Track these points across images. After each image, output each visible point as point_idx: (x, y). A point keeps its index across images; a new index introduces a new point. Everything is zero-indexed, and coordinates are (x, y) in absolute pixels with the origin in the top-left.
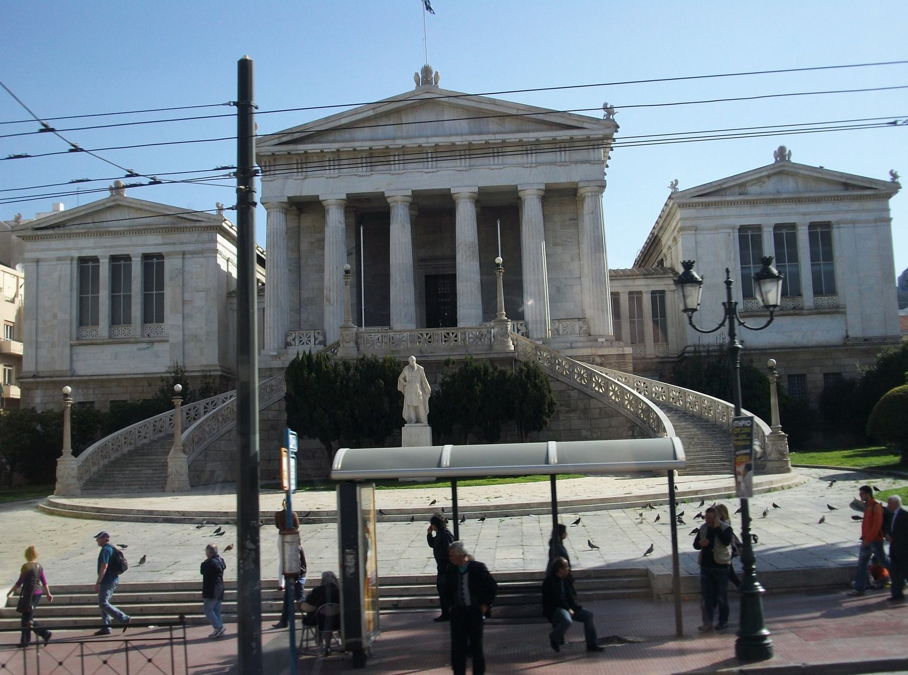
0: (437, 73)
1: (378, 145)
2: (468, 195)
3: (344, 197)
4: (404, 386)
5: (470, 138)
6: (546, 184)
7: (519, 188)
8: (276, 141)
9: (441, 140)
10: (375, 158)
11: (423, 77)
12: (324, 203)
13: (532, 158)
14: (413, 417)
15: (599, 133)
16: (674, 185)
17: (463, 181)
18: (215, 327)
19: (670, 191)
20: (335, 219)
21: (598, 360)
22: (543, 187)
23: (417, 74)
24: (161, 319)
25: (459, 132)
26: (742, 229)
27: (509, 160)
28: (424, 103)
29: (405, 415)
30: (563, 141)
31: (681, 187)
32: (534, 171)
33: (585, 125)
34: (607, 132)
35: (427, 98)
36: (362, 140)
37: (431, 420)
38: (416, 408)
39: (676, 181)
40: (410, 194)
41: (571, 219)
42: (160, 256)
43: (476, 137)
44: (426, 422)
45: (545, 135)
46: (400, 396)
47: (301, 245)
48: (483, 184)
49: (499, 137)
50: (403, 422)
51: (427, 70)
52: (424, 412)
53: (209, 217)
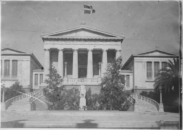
1: (71, 38)
6: (108, 49)
20: (61, 54)
24: (16, 75)
26: (148, 62)
34: (123, 38)
42: (17, 61)
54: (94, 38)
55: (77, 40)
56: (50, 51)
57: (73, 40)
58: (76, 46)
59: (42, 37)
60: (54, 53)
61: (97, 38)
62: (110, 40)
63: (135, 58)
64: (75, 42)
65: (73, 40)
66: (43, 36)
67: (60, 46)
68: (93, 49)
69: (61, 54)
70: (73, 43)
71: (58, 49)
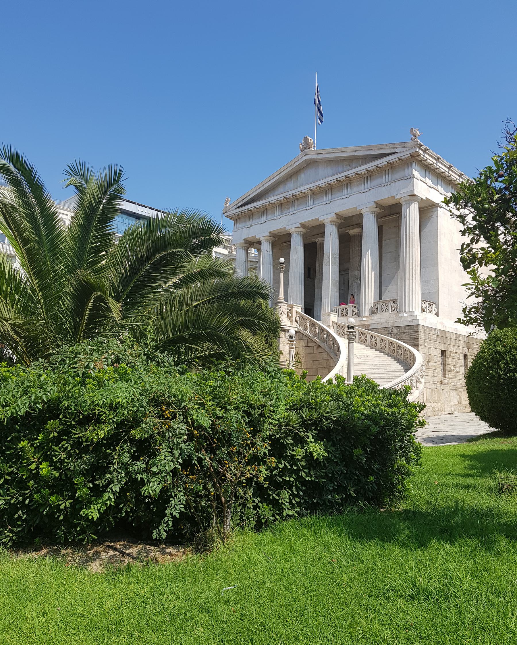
2: (329, 220)
5: (327, 180)
8: (236, 207)
10: (282, 206)
13: (368, 185)
21: (395, 331)
22: (373, 205)
25: (325, 177)
27: (355, 189)
28: (310, 164)
30: (386, 166)
32: (367, 193)
34: (413, 151)
43: (331, 178)
45: (371, 165)
48: (337, 211)
54: (331, 179)
59: (226, 214)
62: (381, 171)
70: (289, 211)
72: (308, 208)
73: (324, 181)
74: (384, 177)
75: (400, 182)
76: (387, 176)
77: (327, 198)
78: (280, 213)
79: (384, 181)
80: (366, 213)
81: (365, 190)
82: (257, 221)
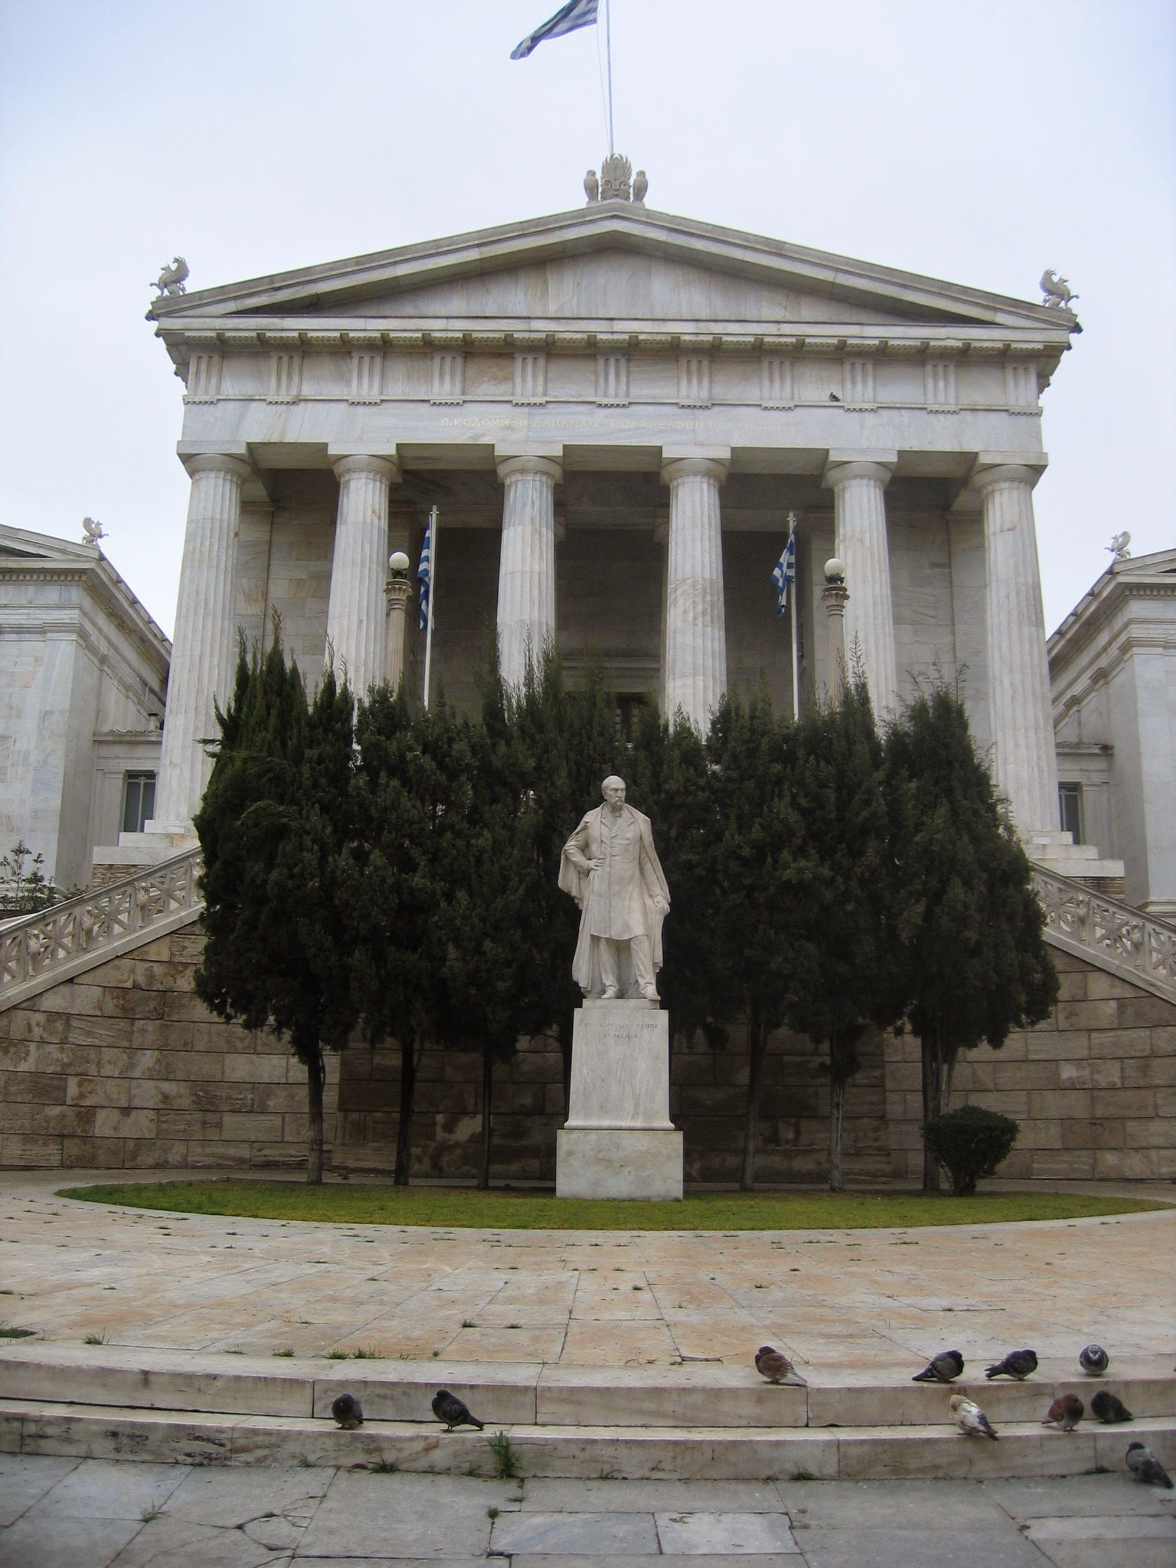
0: (642, 174)
1: (482, 330)
3: (392, 451)
4: (585, 873)
5: (717, 328)
6: (901, 454)
7: (833, 457)
8: (232, 306)
9: (645, 330)
11: (608, 182)
12: (338, 468)
14: (609, 980)
15: (1034, 338)
16: (1119, 548)
17: (694, 429)
18: (55, 801)
19: (1113, 555)
22: (894, 458)
23: (592, 173)
29: (581, 971)
31: (1136, 550)
32: (870, 418)
33: (1001, 318)
34: (1055, 336)
35: (612, 237)
36: (447, 316)
37: (671, 990)
38: (621, 949)
39: (1125, 535)
40: (559, 452)
41: (934, 565)
44: (651, 990)
46: (569, 912)
47: (271, 587)
49: (786, 329)
50: (576, 997)
51: (616, 168)
52: (648, 959)
53: (63, 548)
54: (736, 333)
55: (549, 350)
56: (259, 491)
57: (502, 352)
58: (524, 425)
60: (285, 496)
61: (772, 329)
63: (1137, 608)
64: (528, 381)
65: (502, 352)
66: (168, 314)
67: (361, 422)
68: (725, 454)
69: (363, 505)
71: (333, 451)
72: (604, 401)
73: (702, 328)
74: (930, 383)
75: (992, 415)
76: (941, 384)
77: (693, 389)
78: (458, 385)
79: (930, 395)
80: (855, 482)
81: (865, 406)
82: (334, 390)
